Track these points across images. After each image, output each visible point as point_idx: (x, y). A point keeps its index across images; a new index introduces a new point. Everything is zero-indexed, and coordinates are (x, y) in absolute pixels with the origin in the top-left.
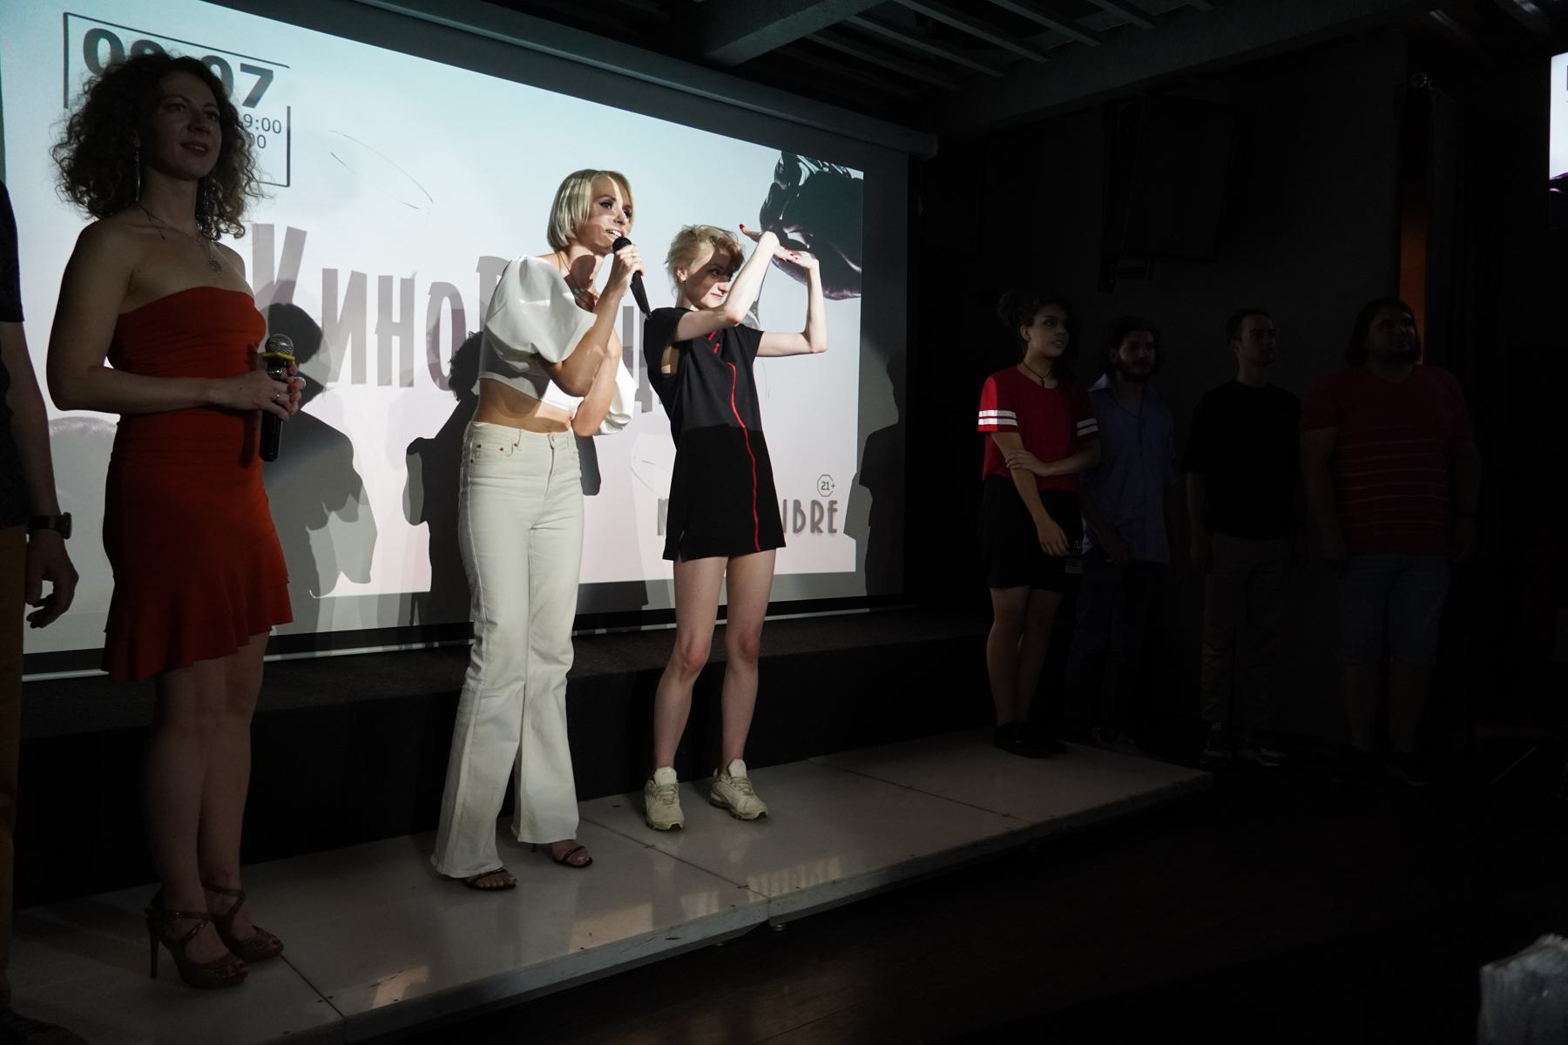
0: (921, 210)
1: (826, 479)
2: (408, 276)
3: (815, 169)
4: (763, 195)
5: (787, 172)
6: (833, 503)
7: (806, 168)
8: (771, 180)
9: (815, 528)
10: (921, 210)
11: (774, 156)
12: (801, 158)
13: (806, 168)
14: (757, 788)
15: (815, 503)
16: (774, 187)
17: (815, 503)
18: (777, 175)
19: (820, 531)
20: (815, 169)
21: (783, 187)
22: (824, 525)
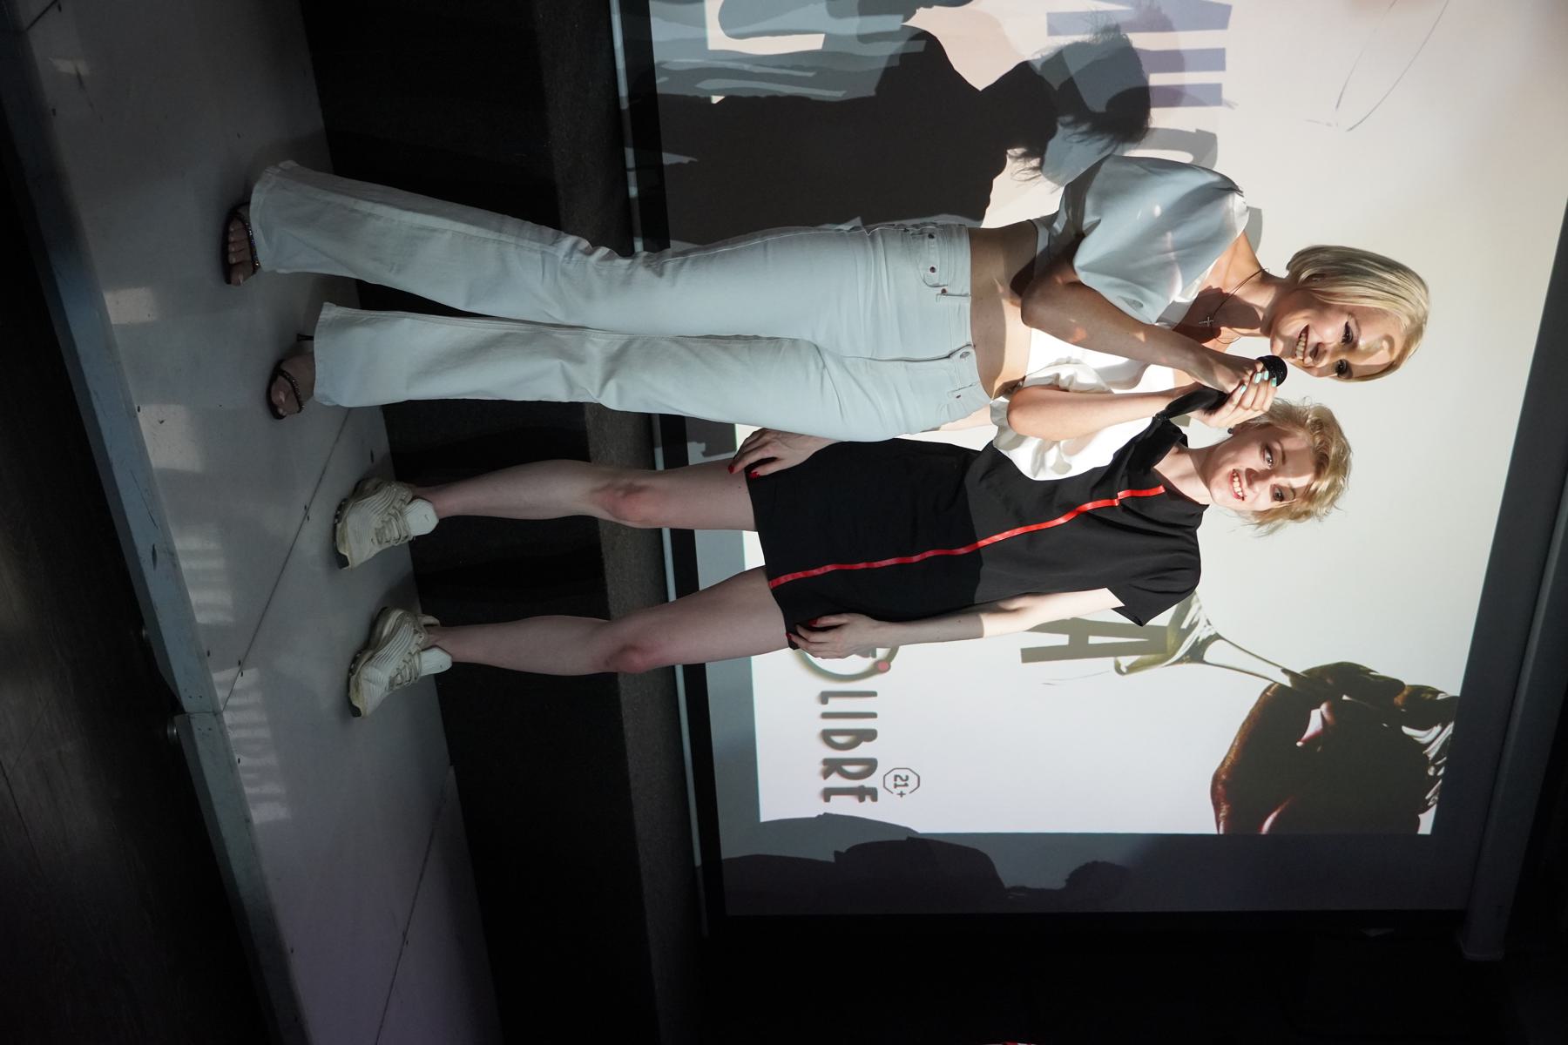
0: (1373, 933)
1: (912, 782)
2: (1225, 95)
3: (1432, 752)
4: (1383, 665)
5: (1424, 705)
6: (873, 794)
7: (1433, 738)
8: (1409, 680)
9: (831, 767)
10: (1373, 933)
11: (1449, 680)
12: (1451, 726)
13: (1433, 738)
14: (406, 691)
15: (871, 765)
16: (1397, 685)
17: (871, 765)
18: (1419, 690)
19: (826, 775)
20: (1432, 752)
21: (1398, 700)
22: (836, 781)
